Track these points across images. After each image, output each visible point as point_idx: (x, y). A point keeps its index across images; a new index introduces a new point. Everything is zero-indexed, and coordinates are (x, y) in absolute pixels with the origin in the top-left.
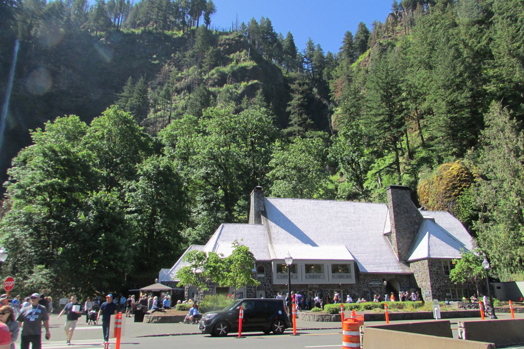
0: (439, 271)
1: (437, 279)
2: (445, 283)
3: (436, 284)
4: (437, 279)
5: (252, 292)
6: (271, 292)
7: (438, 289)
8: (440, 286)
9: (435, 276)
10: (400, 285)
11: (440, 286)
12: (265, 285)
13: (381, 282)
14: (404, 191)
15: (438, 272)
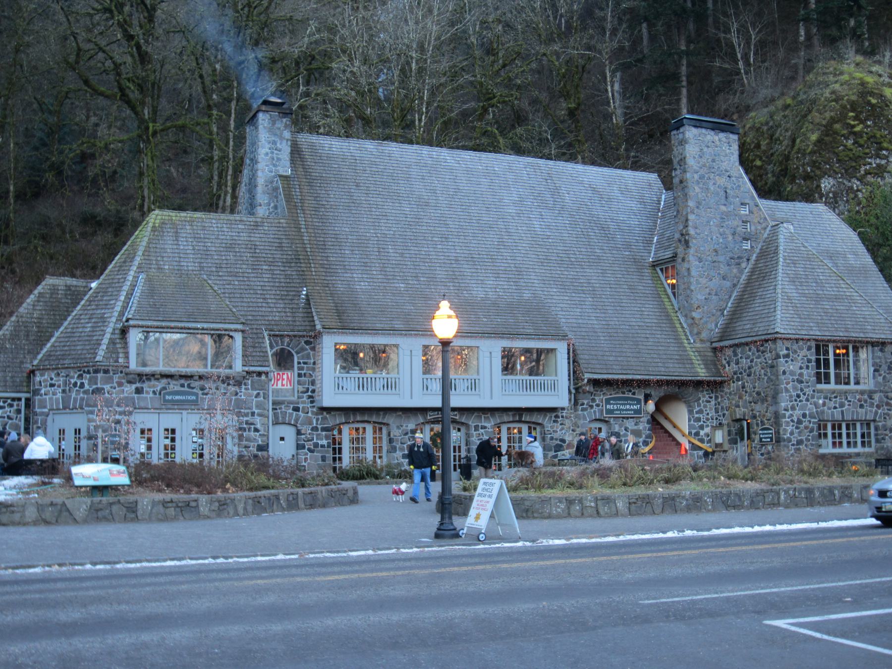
0: (805, 371)
1: (798, 396)
2: (816, 405)
3: (793, 408)
4: (798, 396)
5: (256, 430)
6: (315, 429)
7: (799, 422)
8: (804, 416)
9: (795, 388)
10: (690, 412)
11: (804, 416)
12: (296, 409)
13: (638, 401)
14: (722, 135)
15: (801, 375)
